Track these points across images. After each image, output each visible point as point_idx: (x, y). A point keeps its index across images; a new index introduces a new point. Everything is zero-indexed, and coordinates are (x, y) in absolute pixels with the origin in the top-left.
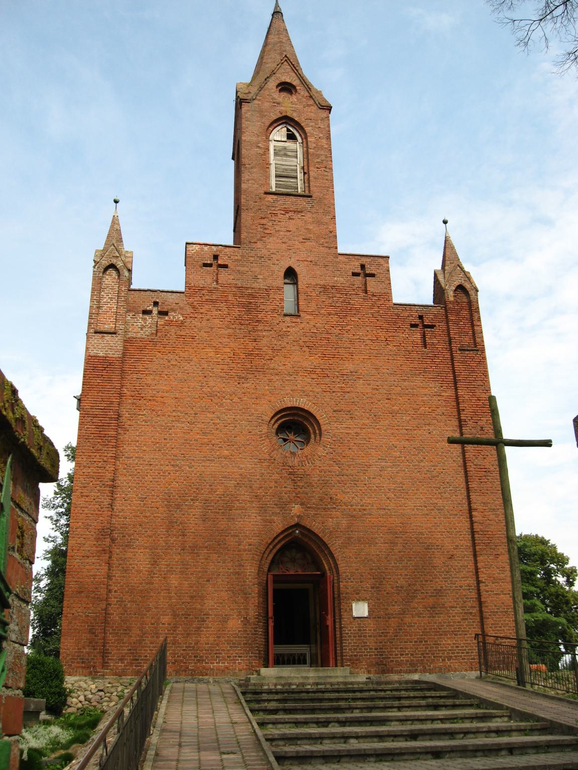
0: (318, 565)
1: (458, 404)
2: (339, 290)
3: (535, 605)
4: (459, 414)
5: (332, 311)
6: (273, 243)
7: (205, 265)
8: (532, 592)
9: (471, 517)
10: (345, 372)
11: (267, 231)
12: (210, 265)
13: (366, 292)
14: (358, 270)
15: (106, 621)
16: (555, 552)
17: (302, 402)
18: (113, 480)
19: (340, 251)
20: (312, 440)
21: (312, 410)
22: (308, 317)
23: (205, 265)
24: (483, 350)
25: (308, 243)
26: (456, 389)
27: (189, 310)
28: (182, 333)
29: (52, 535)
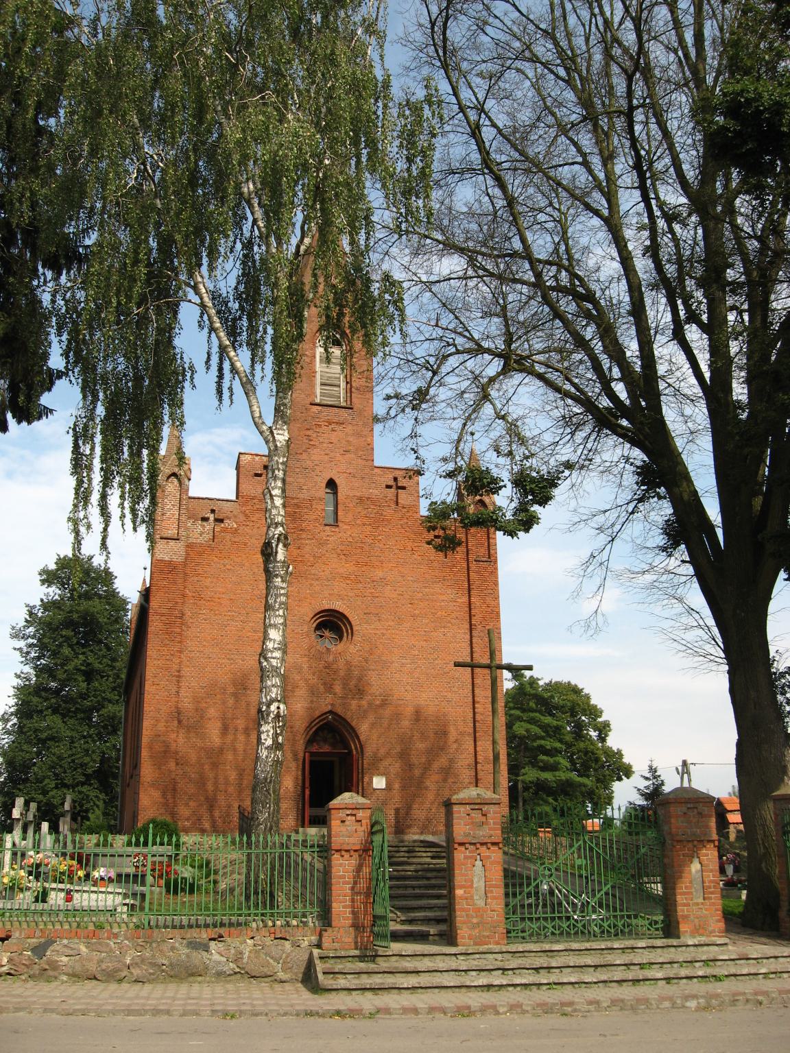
0: (347, 746)
1: (470, 609)
2: (373, 502)
3: (559, 763)
4: (470, 619)
5: (366, 521)
6: (316, 455)
7: (257, 475)
8: (556, 749)
9: (474, 708)
10: (375, 578)
11: (312, 443)
12: (260, 475)
13: (397, 503)
14: (391, 483)
15: (174, 790)
16: (588, 703)
17: (338, 605)
18: (179, 671)
19: (376, 464)
20: (345, 638)
21: (346, 613)
22: (345, 527)
23: (257, 475)
24: (496, 562)
25: (348, 455)
26: (470, 596)
27: (242, 518)
28: (236, 540)
29: (25, 671)
